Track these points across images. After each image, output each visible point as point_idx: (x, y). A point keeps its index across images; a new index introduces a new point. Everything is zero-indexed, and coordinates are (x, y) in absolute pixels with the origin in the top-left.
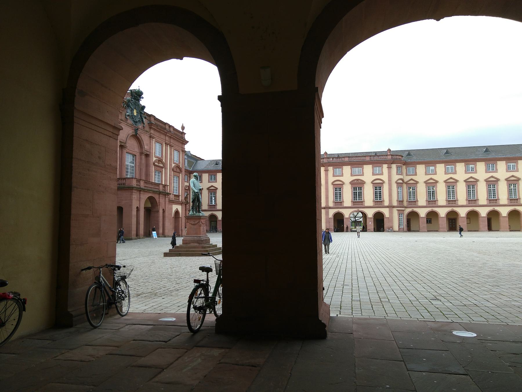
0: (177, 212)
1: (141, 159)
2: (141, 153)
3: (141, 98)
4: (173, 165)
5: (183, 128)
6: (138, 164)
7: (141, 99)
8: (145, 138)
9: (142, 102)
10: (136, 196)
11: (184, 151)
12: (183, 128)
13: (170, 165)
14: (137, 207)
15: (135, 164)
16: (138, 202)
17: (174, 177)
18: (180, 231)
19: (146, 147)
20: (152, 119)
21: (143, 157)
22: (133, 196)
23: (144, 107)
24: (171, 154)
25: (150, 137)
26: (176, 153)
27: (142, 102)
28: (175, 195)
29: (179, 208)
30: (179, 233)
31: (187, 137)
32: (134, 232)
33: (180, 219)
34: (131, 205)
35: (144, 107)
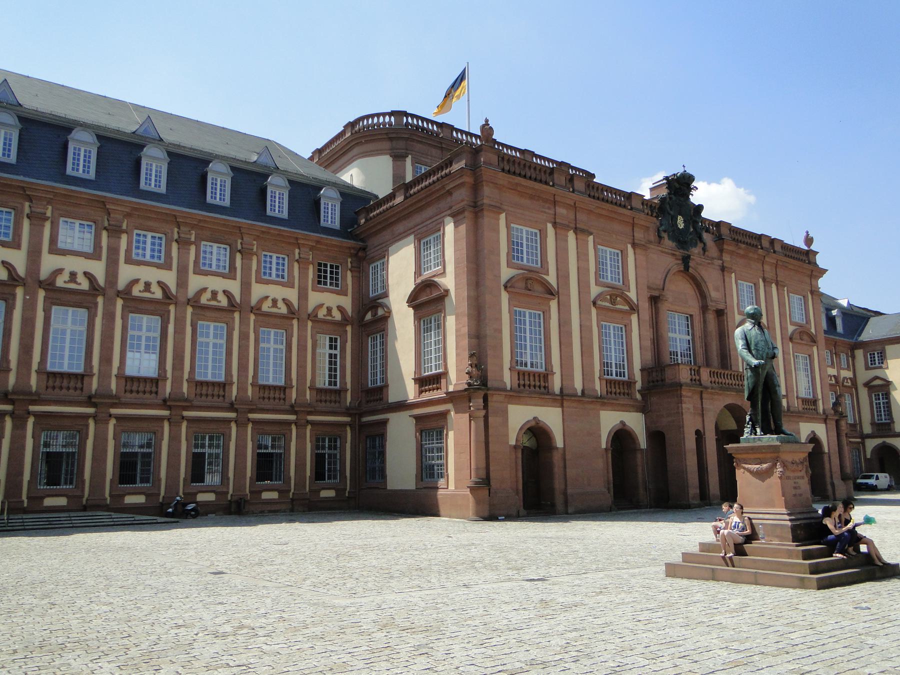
0: (814, 439)
1: (705, 322)
2: (704, 308)
3: (690, 189)
4: (791, 329)
5: (809, 241)
6: (698, 333)
7: (693, 192)
8: (710, 276)
9: (696, 198)
10: (691, 406)
11: (815, 292)
12: (809, 241)
13: (783, 328)
14: (698, 432)
15: (693, 335)
16: (700, 419)
17: (795, 357)
18: (829, 487)
19: (714, 294)
20: (724, 231)
21: (711, 317)
22: (684, 406)
23: (700, 208)
24: (781, 305)
25: (723, 269)
26: (796, 299)
27: (696, 198)
28: (805, 401)
29: (820, 430)
30: (825, 490)
31: (821, 261)
32: (694, 490)
33: (826, 458)
34: (680, 428)
35: (700, 208)
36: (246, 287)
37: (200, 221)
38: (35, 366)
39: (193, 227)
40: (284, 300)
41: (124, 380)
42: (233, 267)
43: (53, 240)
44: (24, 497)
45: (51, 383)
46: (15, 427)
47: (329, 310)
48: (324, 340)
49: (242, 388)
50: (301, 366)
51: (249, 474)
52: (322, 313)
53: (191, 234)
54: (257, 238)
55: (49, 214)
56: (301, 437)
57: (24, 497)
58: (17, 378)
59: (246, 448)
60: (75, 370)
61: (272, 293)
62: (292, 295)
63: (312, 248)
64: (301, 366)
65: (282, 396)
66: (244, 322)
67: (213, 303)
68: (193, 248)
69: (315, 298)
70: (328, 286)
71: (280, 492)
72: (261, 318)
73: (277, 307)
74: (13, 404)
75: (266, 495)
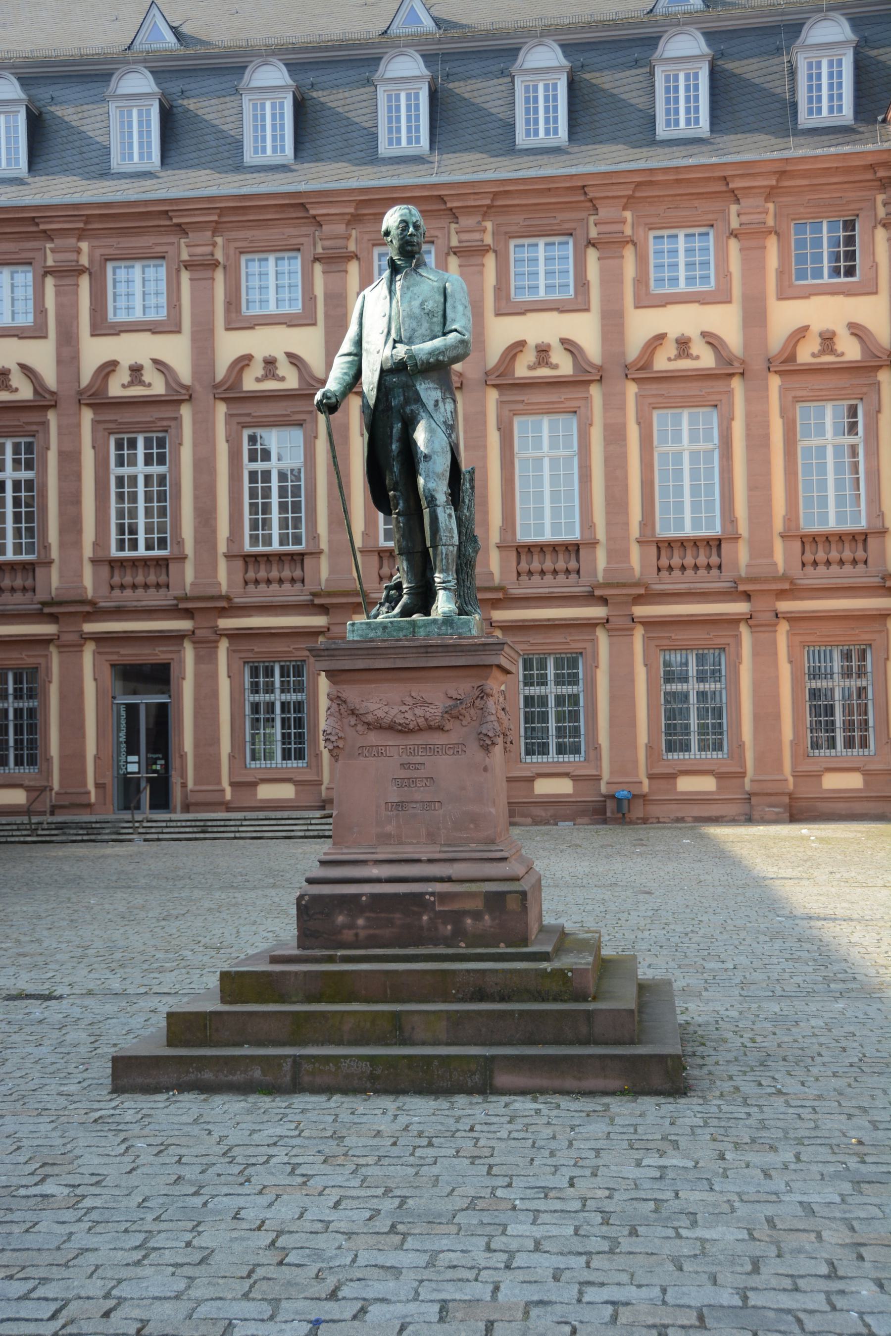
36: (613, 325)
37: (496, 195)
38: (222, 547)
39: (487, 211)
40: (704, 334)
41: (376, 558)
42: (582, 284)
43: (233, 303)
44: (225, 784)
45: (251, 575)
46: (198, 660)
47: (828, 340)
48: (831, 415)
49: (618, 553)
50: (759, 485)
51: (643, 737)
52: (806, 354)
53: (484, 230)
54: (629, 202)
55: (219, 256)
56: (765, 655)
57: (225, 784)
58: (196, 571)
59: (633, 681)
60: (563, 537)
61: (689, 322)
62: (726, 322)
63: (771, 194)
64: (759, 485)
65: (714, 560)
66: (614, 404)
67: (544, 372)
68: (490, 261)
69: (785, 316)
70: (826, 279)
71: (720, 777)
72: (653, 389)
73: (689, 356)
74: (192, 618)
75: (686, 784)
